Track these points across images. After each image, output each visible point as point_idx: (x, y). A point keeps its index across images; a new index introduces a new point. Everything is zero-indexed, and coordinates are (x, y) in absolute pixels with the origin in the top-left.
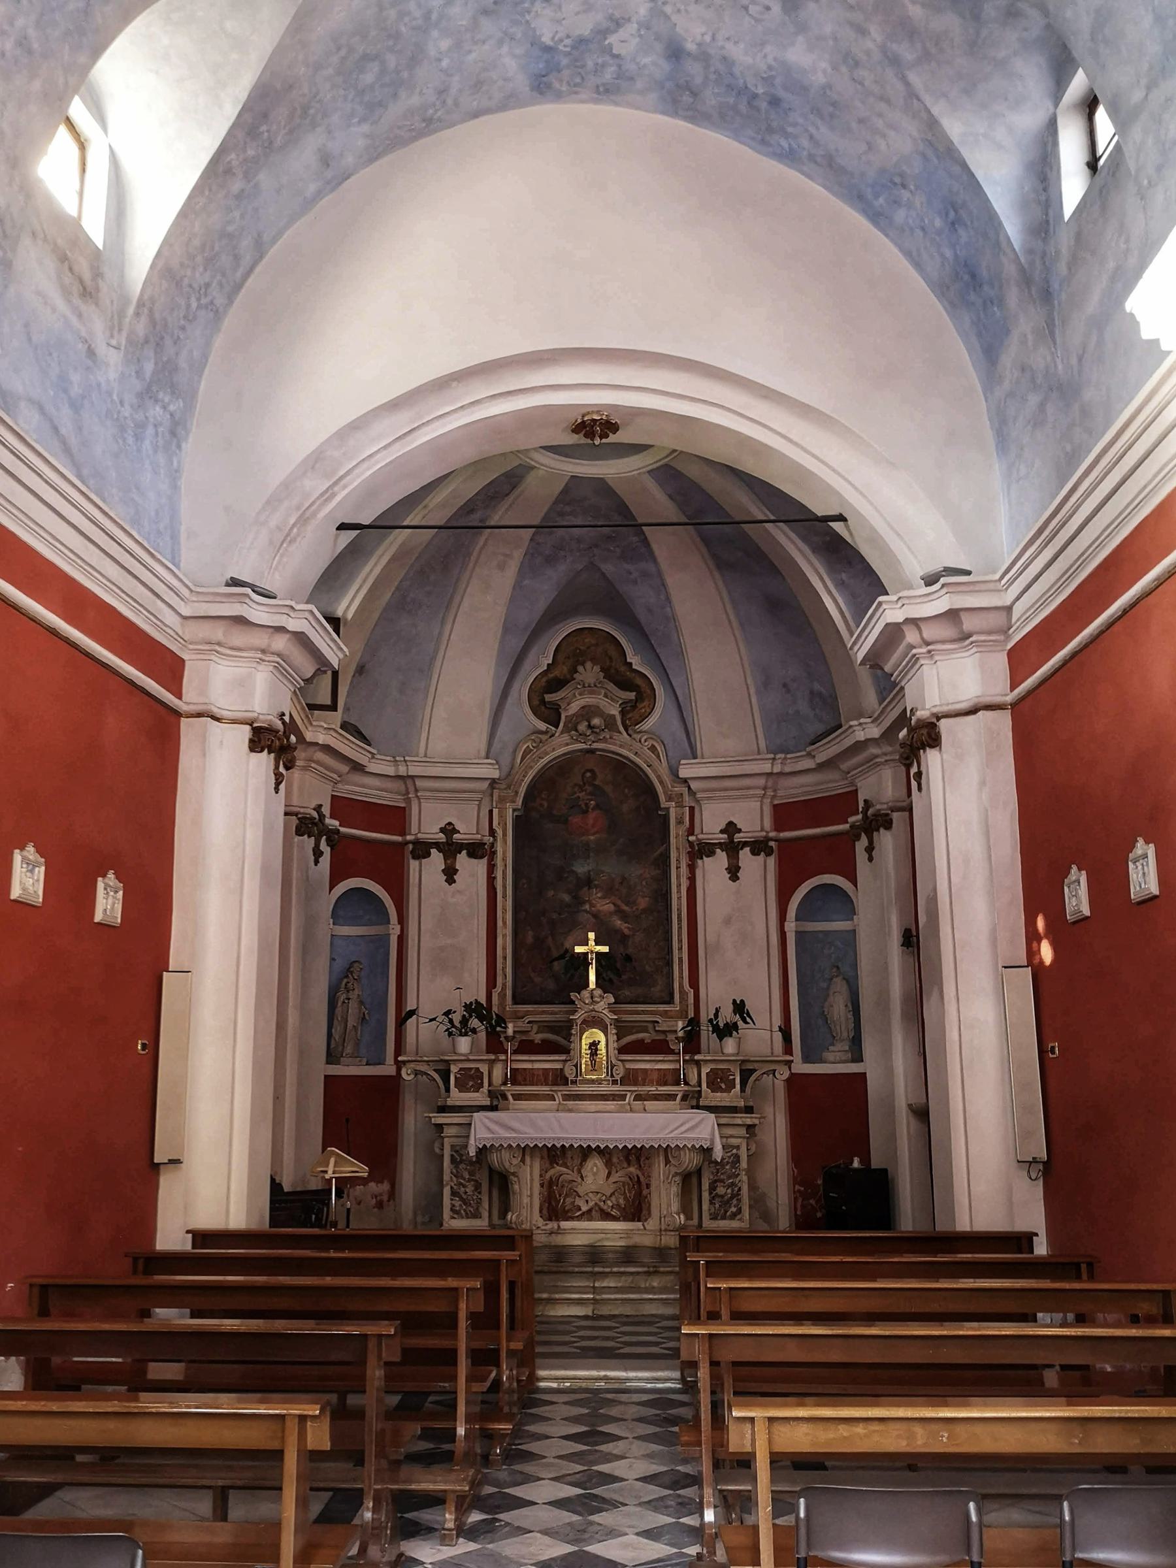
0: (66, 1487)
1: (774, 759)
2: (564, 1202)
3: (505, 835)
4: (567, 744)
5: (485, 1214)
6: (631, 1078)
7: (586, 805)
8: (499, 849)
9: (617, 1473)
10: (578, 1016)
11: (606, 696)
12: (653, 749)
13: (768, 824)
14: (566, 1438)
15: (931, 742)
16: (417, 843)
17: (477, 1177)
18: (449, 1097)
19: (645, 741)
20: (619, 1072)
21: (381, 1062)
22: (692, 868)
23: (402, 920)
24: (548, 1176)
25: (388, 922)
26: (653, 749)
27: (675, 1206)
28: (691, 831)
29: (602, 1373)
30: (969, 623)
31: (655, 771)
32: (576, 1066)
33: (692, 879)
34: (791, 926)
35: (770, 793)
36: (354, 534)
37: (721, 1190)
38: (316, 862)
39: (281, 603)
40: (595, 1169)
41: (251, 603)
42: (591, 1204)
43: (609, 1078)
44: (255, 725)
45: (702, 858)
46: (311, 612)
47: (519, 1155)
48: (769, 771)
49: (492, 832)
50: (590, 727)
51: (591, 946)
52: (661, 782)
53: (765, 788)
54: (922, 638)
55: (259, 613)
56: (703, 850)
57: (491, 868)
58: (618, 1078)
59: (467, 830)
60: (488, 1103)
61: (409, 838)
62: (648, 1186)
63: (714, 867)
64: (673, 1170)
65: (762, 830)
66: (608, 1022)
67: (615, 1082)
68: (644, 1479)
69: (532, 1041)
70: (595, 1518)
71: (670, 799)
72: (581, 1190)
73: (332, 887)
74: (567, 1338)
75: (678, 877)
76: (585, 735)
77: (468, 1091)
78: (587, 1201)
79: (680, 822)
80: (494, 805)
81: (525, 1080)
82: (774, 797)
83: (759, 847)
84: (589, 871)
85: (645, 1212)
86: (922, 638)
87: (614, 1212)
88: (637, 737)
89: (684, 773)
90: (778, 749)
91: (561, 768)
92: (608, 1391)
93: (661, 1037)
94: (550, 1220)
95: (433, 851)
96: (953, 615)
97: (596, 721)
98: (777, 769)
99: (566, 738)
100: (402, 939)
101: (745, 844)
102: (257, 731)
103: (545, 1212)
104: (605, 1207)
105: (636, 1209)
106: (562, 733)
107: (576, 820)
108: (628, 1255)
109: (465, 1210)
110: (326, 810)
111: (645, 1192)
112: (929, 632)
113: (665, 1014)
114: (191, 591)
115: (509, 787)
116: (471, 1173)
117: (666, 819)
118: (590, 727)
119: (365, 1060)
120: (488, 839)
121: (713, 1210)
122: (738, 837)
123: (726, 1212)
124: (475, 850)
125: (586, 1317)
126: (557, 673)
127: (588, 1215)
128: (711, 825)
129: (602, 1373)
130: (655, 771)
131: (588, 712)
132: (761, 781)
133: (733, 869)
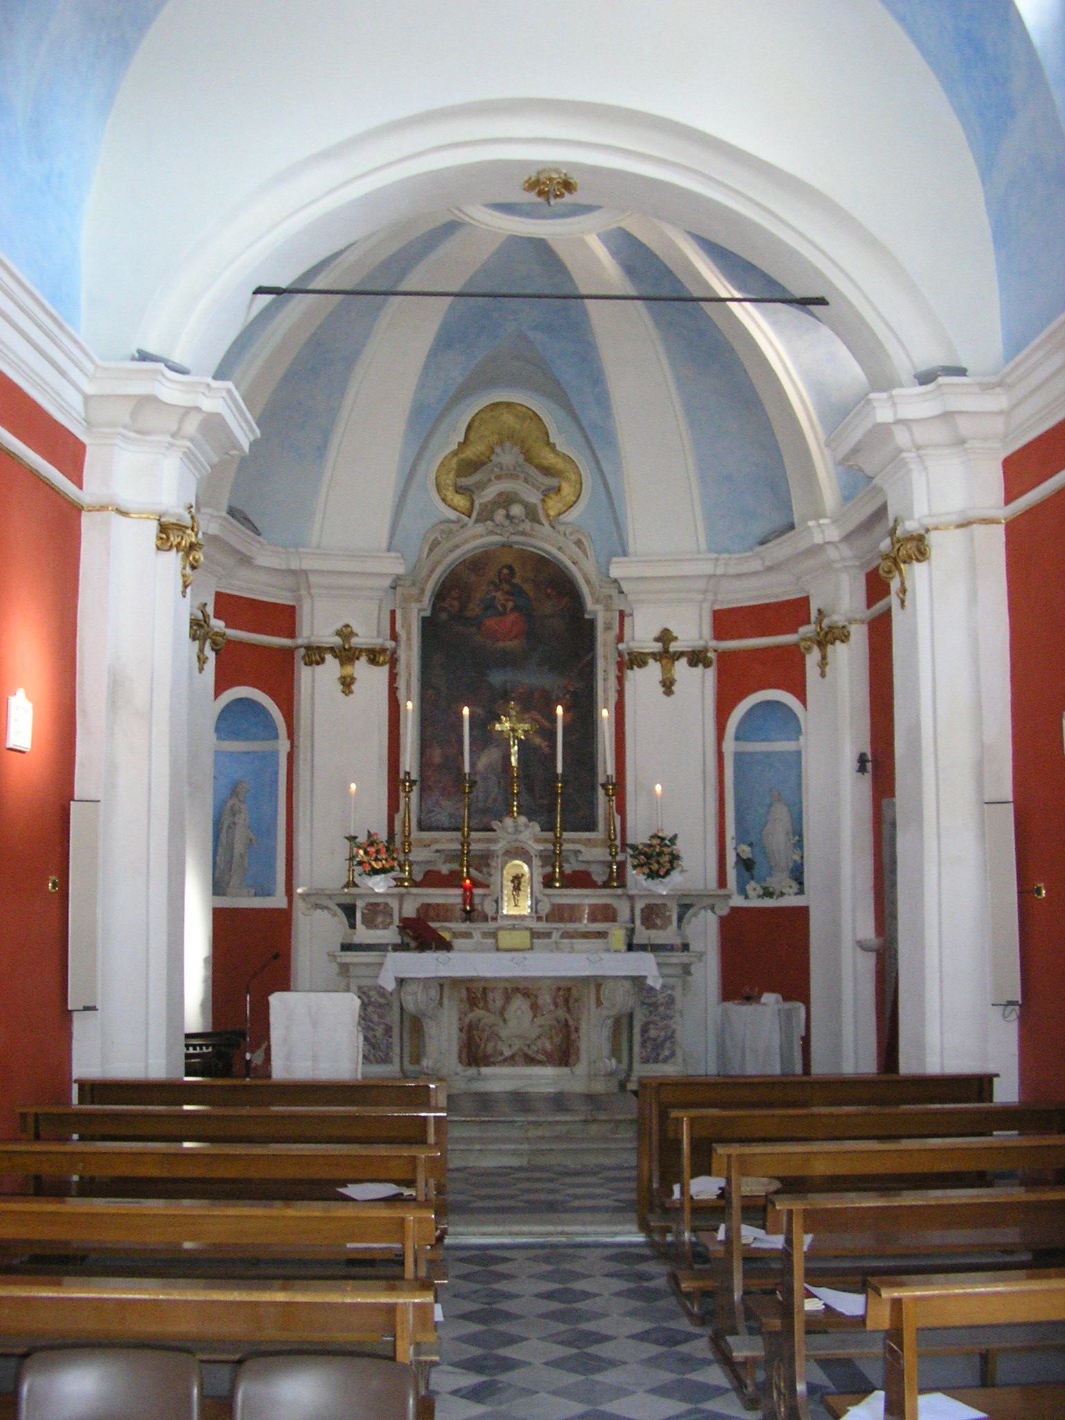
0: (42, 1355)
1: (717, 560)
2: (485, 1048)
3: (409, 639)
4: (482, 536)
5: (397, 1060)
6: (560, 914)
7: (504, 606)
8: (402, 654)
9: (604, 1331)
10: (499, 847)
11: (526, 481)
12: (579, 543)
13: (707, 631)
14: (540, 1296)
15: (919, 557)
16: (308, 648)
17: (387, 1020)
18: (355, 934)
19: (571, 534)
20: (545, 908)
21: (269, 893)
22: (620, 680)
23: (291, 735)
24: (467, 1020)
25: (276, 737)
26: (579, 543)
27: (606, 1048)
28: (620, 639)
29: (559, 1229)
30: (965, 426)
31: (580, 569)
32: (497, 901)
33: (621, 693)
34: (729, 746)
35: (710, 597)
36: (269, 298)
37: (653, 1033)
38: (201, 670)
39: (197, 379)
40: (519, 1012)
41: (163, 380)
42: (515, 1048)
43: (534, 915)
44: (163, 520)
45: (632, 669)
46: (229, 391)
47: (434, 993)
48: (712, 572)
49: (394, 636)
50: (508, 516)
51: (560, 785)
52: (588, 582)
53: (705, 592)
54: (913, 441)
55: (171, 391)
56: (637, 660)
57: (393, 677)
58: (543, 914)
59: (365, 636)
60: (399, 941)
61: (300, 641)
62: (577, 1030)
63: (645, 680)
64: (605, 1012)
65: (701, 638)
66: (532, 853)
67: (539, 919)
68: (606, 1338)
69: (439, 872)
70: (599, 1377)
71: (597, 601)
72: (504, 1033)
73: (217, 694)
74: (507, 1192)
75: (605, 691)
76: (503, 526)
77: (376, 927)
78: (510, 1046)
79: (608, 628)
80: (398, 606)
81: (438, 915)
82: (715, 602)
83: (696, 658)
84: (506, 681)
85: (573, 1057)
86: (913, 441)
87: (541, 1057)
88: (562, 528)
89: (615, 572)
90: (717, 549)
91: (477, 563)
92: (567, 1246)
93: (582, 868)
94: (470, 1064)
95: (329, 657)
96: (947, 416)
97: (516, 510)
98: (720, 571)
99: (480, 528)
100: (291, 756)
101: (682, 654)
102: (164, 528)
103: (464, 1056)
104: (530, 1053)
105: (564, 1055)
106: (477, 521)
107: (490, 623)
108: (559, 1102)
109: (374, 1056)
110: (210, 610)
111: (574, 1036)
112: (921, 434)
113: (588, 843)
114: (97, 366)
115: (414, 584)
116: (381, 1016)
117: (592, 623)
118: (508, 516)
119: (253, 891)
120: (390, 644)
121: (644, 1054)
122: (674, 647)
123: (658, 1055)
124: (374, 656)
125: (520, 1169)
126: (469, 453)
127: (511, 1060)
128: (642, 635)
129: (559, 1229)
130: (580, 569)
131: (506, 500)
132: (701, 584)
133: (668, 683)
